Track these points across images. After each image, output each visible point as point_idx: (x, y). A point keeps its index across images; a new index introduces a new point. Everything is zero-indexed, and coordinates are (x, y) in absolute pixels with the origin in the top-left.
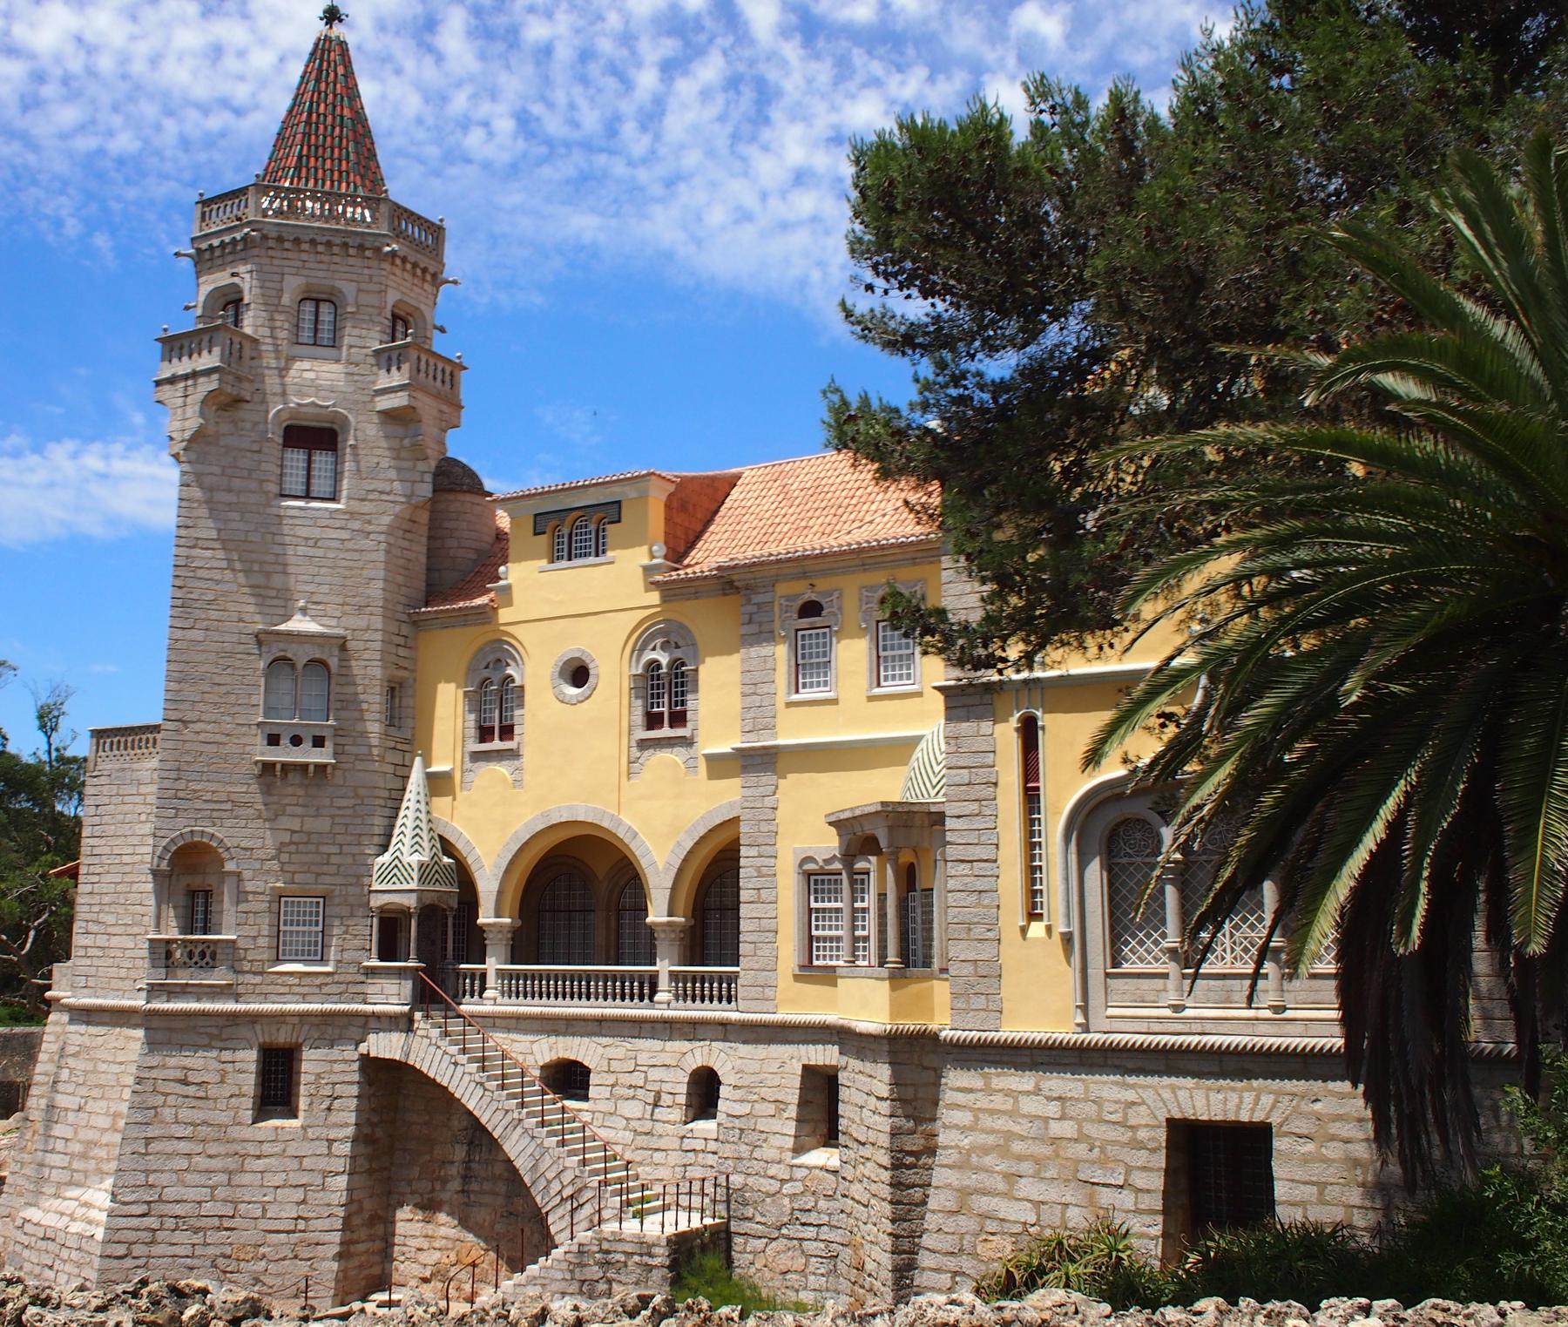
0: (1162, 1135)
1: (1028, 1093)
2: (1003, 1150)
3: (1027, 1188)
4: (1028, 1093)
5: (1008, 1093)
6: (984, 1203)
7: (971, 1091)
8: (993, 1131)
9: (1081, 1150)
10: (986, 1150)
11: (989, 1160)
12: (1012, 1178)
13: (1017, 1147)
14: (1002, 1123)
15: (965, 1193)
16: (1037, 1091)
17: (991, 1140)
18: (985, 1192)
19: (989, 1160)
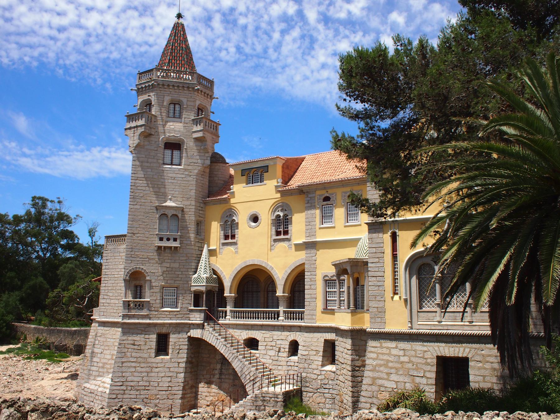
1: (394, 348)
2: (386, 366)
4: (394, 348)
5: (388, 348)
6: (380, 382)
7: (376, 347)
8: (383, 360)
9: (410, 365)
10: (381, 366)
11: (382, 369)
13: (390, 365)
14: (386, 357)
15: (374, 379)
16: (396, 347)
17: (382, 362)
18: (380, 379)
19: (382, 369)
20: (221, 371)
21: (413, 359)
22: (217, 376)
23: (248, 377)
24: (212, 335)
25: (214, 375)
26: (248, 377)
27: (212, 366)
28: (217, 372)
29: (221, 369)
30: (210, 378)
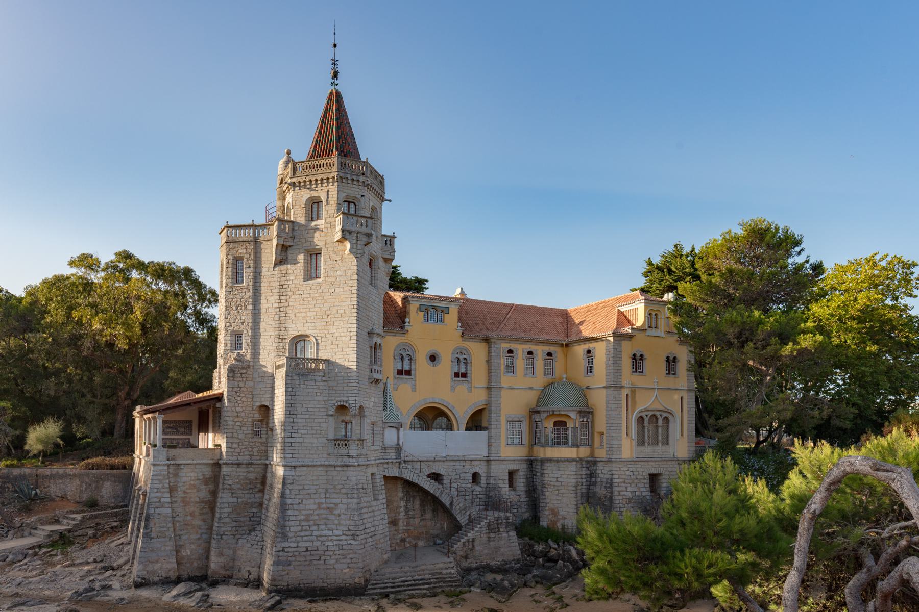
0: (648, 476)
2: (625, 483)
3: (629, 489)
5: (624, 471)
6: (622, 493)
10: (621, 483)
12: (626, 487)
14: (623, 477)
15: (619, 492)
17: (622, 480)
20: (407, 508)
21: (638, 477)
22: (403, 513)
23: (458, 507)
24: (412, 473)
25: (399, 513)
26: (458, 507)
27: (395, 504)
28: (402, 509)
29: (406, 507)
30: (395, 516)
